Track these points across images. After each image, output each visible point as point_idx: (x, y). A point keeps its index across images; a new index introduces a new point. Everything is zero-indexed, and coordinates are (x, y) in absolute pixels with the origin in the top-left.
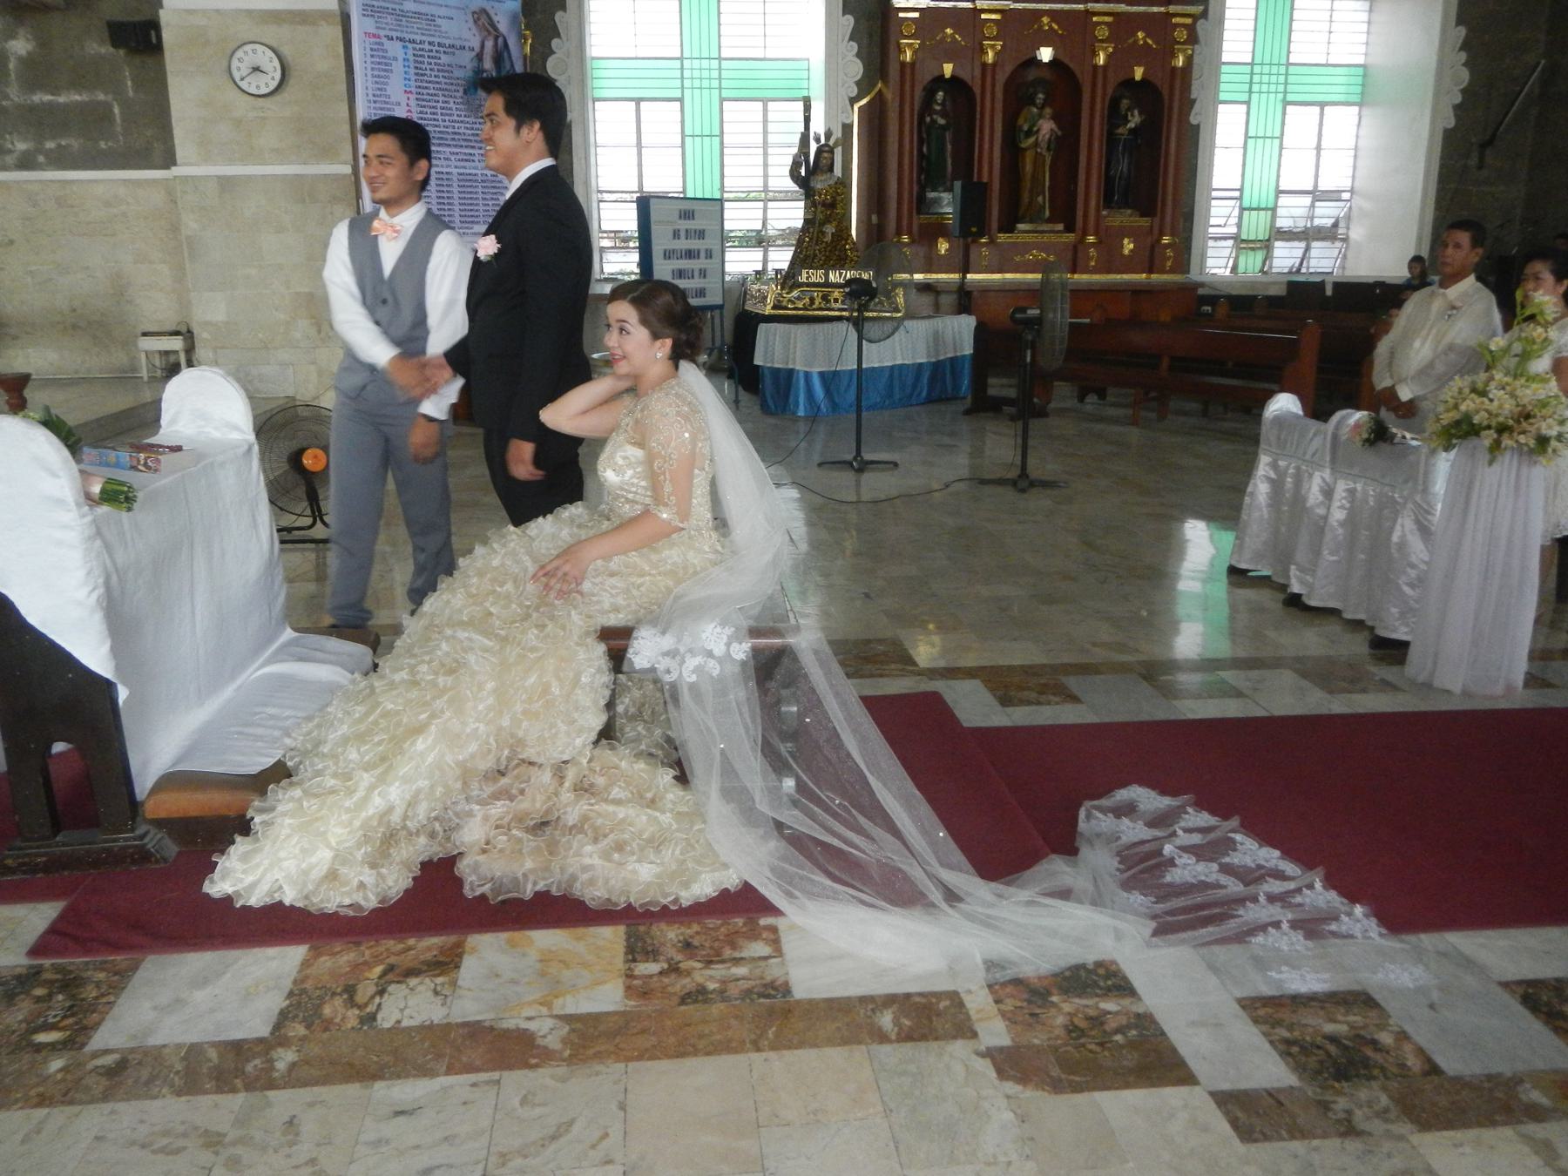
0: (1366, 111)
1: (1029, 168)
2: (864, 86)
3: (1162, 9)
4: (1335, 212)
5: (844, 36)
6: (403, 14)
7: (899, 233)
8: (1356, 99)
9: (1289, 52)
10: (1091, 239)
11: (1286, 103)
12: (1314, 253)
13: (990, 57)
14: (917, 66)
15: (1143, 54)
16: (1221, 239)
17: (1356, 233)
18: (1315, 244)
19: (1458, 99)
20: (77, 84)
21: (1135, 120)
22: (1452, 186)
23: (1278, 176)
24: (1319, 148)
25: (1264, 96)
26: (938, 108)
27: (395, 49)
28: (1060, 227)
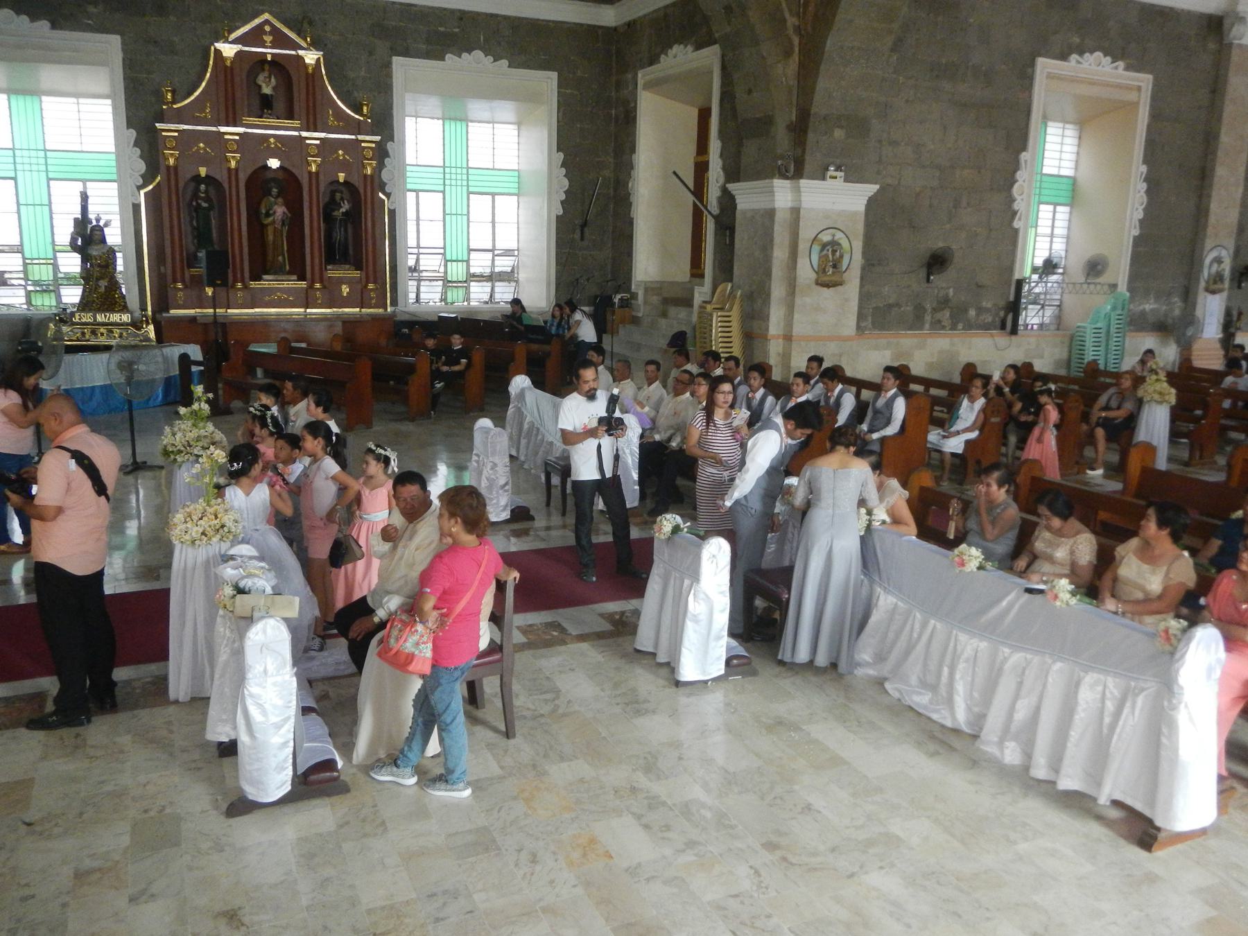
1: (271, 238)
2: (147, 178)
3: (353, 137)
4: (511, 263)
5: (129, 143)
7: (175, 281)
8: (515, 191)
9: (468, 160)
10: (318, 285)
11: (469, 193)
12: (497, 289)
13: (233, 164)
14: (180, 168)
15: (344, 166)
16: (434, 280)
17: (522, 276)
18: (497, 284)
19: (563, 197)
21: (345, 207)
22: (567, 251)
23: (468, 240)
24: (493, 222)
25: (454, 188)
26: (203, 195)
28: (295, 277)
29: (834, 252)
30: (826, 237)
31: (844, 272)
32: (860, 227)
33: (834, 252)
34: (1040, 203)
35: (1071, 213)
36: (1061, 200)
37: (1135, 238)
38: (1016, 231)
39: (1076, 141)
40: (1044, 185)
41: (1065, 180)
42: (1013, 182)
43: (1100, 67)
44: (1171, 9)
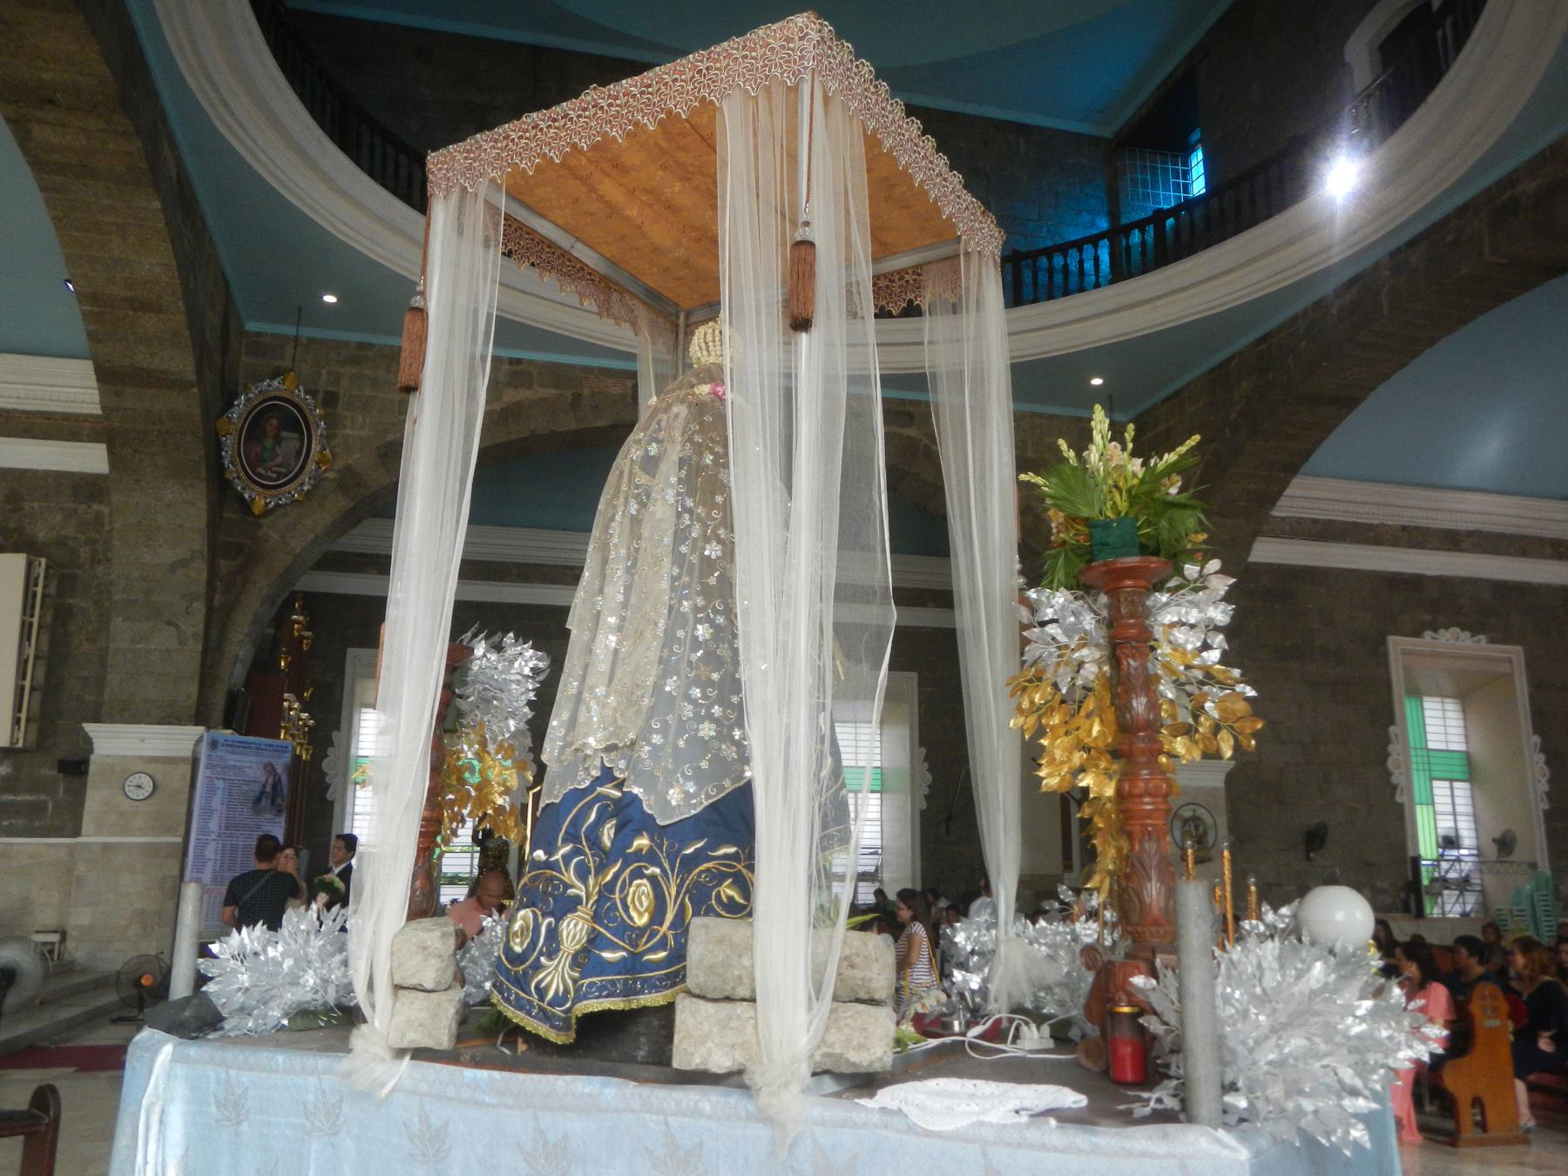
0: (885, 796)
4: (875, 862)
6: (227, 767)
8: (878, 788)
19: (927, 791)
20: (29, 791)
27: (220, 784)
29: (1197, 827)
30: (1187, 813)
31: (1212, 847)
32: (1222, 803)
33: (1197, 827)
34: (1432, 779)
35: (1472, 790)
36: (1458, 776)
37: (1545, 812)
38: (1401, 807)
39: (1459, 715)
40: (1433, 760)
41: (1456, 755)
42: (1386, 756)
43: (1459, 643)
44: (1528, 584)
